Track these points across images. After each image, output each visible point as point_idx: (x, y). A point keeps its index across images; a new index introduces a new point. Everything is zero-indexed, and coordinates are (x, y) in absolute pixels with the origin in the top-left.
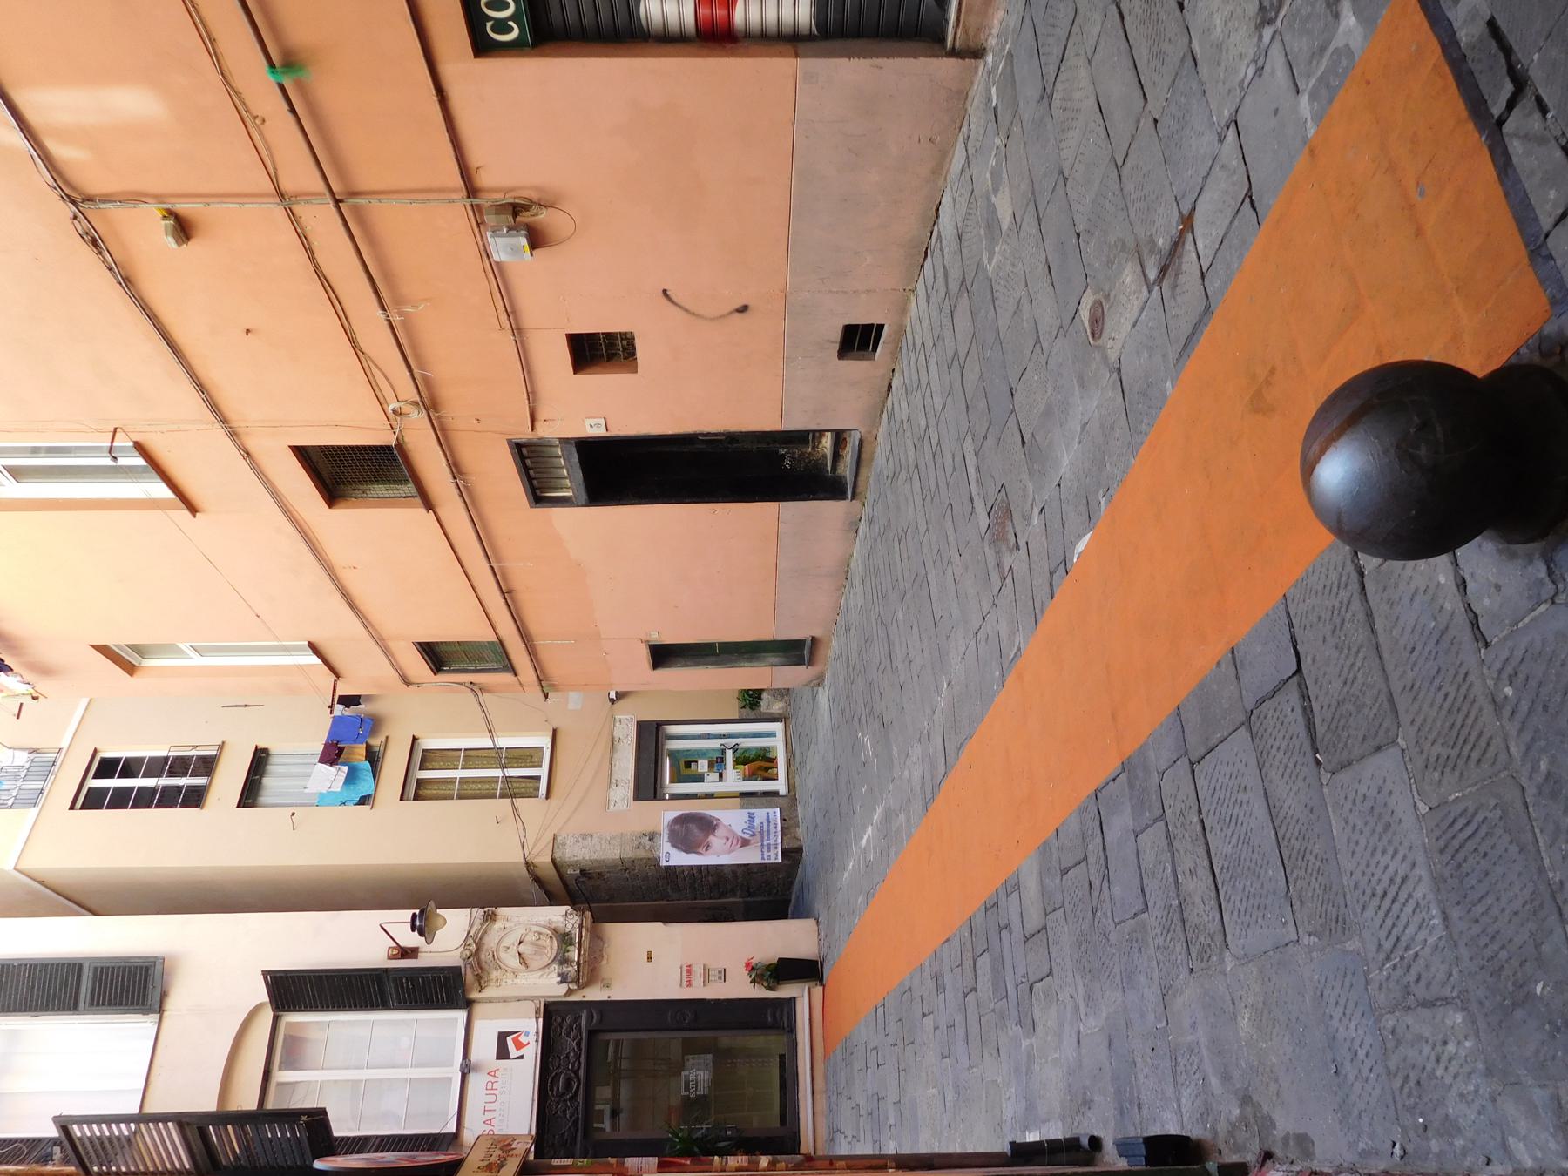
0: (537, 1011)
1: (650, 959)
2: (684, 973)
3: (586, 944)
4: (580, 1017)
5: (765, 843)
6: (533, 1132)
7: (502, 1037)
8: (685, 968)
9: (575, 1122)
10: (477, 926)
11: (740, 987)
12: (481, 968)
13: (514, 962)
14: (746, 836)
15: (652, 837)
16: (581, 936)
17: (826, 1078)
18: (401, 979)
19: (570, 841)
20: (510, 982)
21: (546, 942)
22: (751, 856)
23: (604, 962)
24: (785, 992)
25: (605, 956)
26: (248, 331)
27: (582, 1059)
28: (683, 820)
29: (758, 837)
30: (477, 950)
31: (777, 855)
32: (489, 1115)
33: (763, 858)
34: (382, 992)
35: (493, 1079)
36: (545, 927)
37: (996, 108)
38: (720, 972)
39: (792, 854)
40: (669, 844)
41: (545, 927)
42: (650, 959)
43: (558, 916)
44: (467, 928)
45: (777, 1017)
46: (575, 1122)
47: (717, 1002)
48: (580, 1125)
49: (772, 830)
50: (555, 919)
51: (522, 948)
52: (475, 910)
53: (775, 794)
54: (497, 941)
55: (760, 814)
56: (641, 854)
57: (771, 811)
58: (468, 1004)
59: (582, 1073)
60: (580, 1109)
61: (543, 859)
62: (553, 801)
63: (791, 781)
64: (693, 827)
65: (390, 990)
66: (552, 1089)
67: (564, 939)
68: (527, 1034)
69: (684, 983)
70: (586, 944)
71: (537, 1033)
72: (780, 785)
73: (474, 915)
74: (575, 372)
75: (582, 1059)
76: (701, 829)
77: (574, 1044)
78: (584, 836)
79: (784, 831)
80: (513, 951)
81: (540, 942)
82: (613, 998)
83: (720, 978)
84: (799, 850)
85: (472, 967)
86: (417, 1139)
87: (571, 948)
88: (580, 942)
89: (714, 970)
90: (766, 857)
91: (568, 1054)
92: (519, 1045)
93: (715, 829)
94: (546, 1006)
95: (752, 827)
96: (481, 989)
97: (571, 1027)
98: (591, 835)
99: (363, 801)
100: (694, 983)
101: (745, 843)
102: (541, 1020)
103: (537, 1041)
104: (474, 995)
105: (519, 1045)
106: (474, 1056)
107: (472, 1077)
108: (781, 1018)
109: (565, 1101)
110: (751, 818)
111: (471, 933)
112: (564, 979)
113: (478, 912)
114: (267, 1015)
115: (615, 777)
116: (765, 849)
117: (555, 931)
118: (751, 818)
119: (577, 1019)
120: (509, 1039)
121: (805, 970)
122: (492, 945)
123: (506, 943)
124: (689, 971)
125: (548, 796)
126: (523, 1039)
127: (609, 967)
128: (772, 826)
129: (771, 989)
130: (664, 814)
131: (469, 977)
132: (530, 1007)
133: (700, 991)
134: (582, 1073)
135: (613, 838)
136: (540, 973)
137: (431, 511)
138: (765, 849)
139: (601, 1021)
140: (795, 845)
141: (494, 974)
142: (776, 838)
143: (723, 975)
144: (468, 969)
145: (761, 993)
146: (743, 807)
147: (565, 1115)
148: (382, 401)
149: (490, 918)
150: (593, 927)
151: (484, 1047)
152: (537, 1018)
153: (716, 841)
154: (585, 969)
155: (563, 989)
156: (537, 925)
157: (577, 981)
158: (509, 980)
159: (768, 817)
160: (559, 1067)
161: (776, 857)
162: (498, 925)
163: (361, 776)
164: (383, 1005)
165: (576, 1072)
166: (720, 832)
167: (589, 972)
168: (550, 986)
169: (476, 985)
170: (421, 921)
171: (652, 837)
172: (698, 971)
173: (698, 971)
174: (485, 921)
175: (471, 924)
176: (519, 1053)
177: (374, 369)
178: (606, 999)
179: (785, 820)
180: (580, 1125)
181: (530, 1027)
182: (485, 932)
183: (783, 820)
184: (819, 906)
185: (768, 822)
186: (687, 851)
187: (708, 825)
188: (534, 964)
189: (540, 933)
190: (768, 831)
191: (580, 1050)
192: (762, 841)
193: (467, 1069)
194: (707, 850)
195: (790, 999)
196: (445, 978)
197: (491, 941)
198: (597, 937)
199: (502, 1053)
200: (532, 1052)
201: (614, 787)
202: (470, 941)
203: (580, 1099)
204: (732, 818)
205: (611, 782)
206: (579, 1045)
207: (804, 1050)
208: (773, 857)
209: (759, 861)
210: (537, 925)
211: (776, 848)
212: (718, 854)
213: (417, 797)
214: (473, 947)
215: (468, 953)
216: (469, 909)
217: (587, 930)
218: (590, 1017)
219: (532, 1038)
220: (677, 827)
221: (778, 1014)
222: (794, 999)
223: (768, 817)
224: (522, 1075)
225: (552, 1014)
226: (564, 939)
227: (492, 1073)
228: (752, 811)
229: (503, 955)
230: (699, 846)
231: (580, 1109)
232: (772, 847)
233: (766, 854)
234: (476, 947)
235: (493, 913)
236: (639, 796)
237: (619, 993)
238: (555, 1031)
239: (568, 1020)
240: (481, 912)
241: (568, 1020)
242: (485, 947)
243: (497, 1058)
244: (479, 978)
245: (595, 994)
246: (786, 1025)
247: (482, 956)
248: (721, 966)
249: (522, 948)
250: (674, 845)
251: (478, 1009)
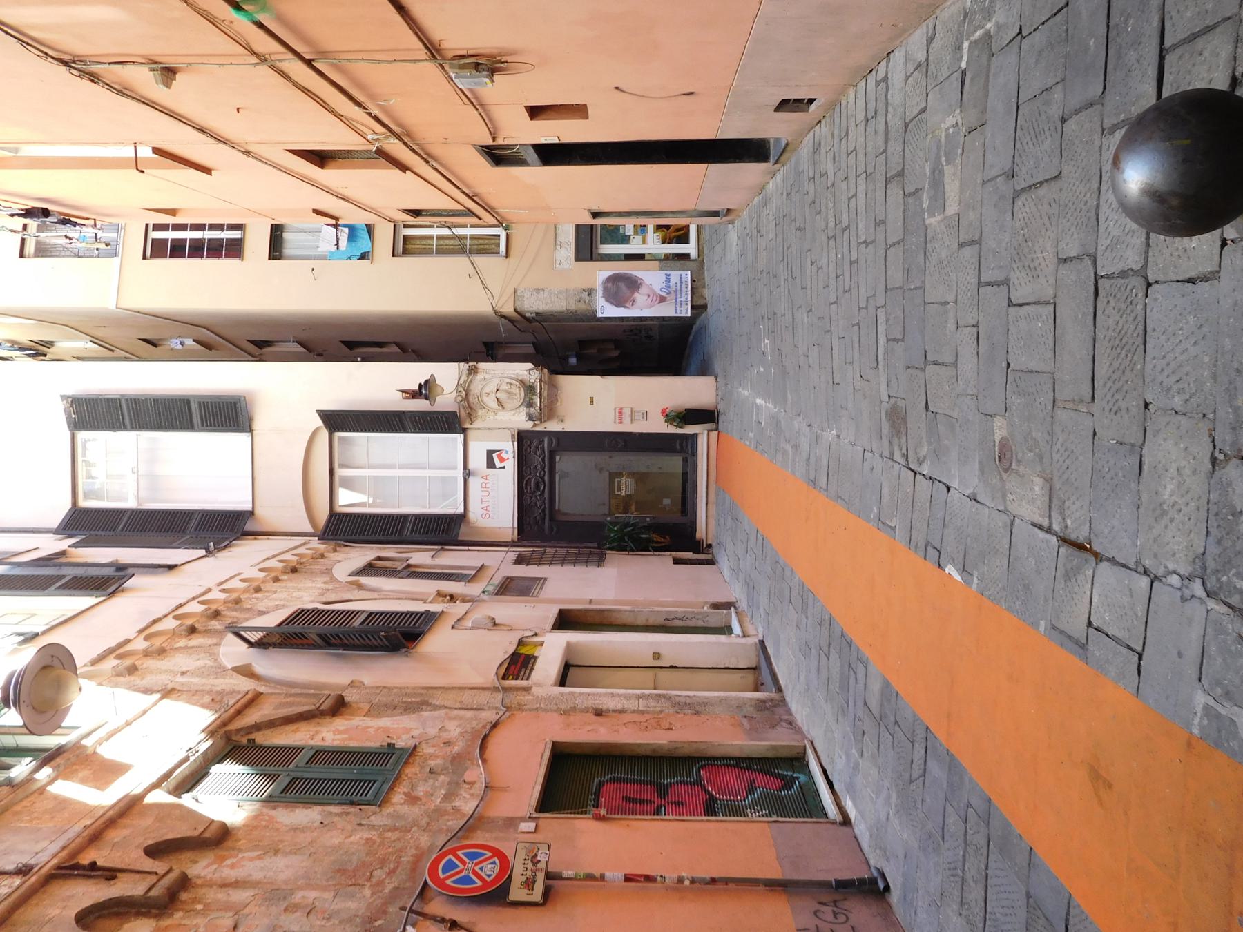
0: (513, 437)
1: (592, 402)
2: (617, 414)
3: (545, 394)
4: (543, 440)
5: (679, 300)
6: (516, 525)
7: (490, 454)
8: (617, 411)
9: (544, 511)
10: (464, 378)
11: (658, 425)
12: (470, 408)
13: (494, 405)
14: (664, 294)
15: (590, 292)
16: (541, 389)
17: (717, 495)
18: (415, 417)
19: (527, 294)
20: (491, 417)
21: (515, 390)
22: (666, 311)
23: (559, 404)
24: (689, 430)
25: (559, 400)
26: (238, 109)
27: (546, 470)
28: (615, 279)
29: (673, 296)
30: (466, 395)
31: (687, 309)
32: (485, 504)
33: (676, 313)
34: (402, 423)
35: (486, 481)
36: (513, 379)
37: (964, 73)
38: (643, 414)
39: (699, 308)
40: (603, 299)
41: (513, 379)
42: (592, 402)
43: (524, 370)
44: (457, 377)
45: (685, 446)
46: (544, 511)
47: (641, 434)
48: (547, 512)
49: (684, 289)
50: (521, 373)
51: (498, 395)
52: (462, 364)
53: (685, 257)
54: (480, 388)
55: (675, 276)
56: (582, 307)
57: (683, 273)
58: (464, 431)
59: (546, 478)
60: (546, 501)
61: (508, 309)
62: (511, 259)
63: (701, 248)
64: (622, 286)
65: (407, 422)
66: (526, 488)
67: (530, 389)
68: (507, 452)
69: (617, 421)
70: (545, 394)
71: (514, 452)
72: (691, 248)
73: (461, 368)
74: (531, 119)
75: (546, 470)
76: (629, 287)
77: (540, 459)
78: (538, 290)
79: (693, 290)
80: (493, 396)
81: (511, 390)
82: (566, 430)
83: (643, 418)
84: (705, 307)
85: (464, 408)
86: (439, 519)
87: (534, 397)
88: (540, 392)
89: (639, 412)
90: (678, 311)
91: (536, 466)
92: (502, 460)
93: (639, 287)
94: (518, 433)
95: (668, 286)
96: (472, 422)
97: (537, 447)
98: (543, 290)
99: (363, 257)
100: (624, 421)
101: (663, 300)
102: (516, 443)
103: (514, 457)
104: (467, 426)
105: (502, 460)
106: (471, 466)
107: (471, 480)
108: (687, 446)
109: (536, 496)
110: (668, 278)
111: (461, 382)
112: (531, 418)
113: (464, 366)
114: (325, 434)
115: (559, 239)
116: (678, 306)
117: (522, 382)
118: (668, 278)
119: (541, 442)
120: (495, 455)
121: (706, 416)
122: (476, 391)
123: (487, 390)
124: (621, 413)
125: (507, 256)
126: (504, 455)
127: (562, 407)
128: (684, 286)
129: (678, 426)
130: (600, 273)
131: (463, 414)
132: (508, 434)
133: (628, 427)
134: (546, 478)
135: (560, 292)
136: (513, 412)
137: (407, 172)
138: (678, 306)
139: (558, 444)
140: (700, 302)
141: (480, 412)
142: (687, 297)
143: (645, 415)
144: (462, 409)
145: (672, 430)
146: (661, 269)
147: (536, 505)
148: (361, 133)
149: (473, 371)
150: (549, 378)
151: (478, 460)
152: (513, 442)
153: (640, 297)
154: (545, 411)
155: (531, 423)
156: (508, 377)
157: (541, 420)
158: (491, 416)
159: (681, 278)
160: (530, 474)
161: (686, 312)
162: (480, 376)
163: (359, 234)
164: (404, 430)
165: (542, 478)
166: (643, 290)
167: (549, 411)
168: (521, 421)
169: (468, 420)
170: (425, 390)
171: (590, 292)
172: (627, 412)
173: (627, 412)
174: (470, 374)
175: (460, 376)
176: (502, 465)
177: (356, 125)
178: (561, 430)
179: (694, 281)
180: (547, 512)
181: (509, 448)
182: (471, 381)
183: (693, 281)
184: (718, 366)
185: (681, 282)
186: (618, 305)
187: (633, 284)
188: (507, 406)
189: (511, 384)
190: (681, 290)
191: (544, 463)
192: (676, 298)
193: (467, 473)
194: (632, 305)
195: (694, 434)
196: (446, 418)
197: (476, 388)
198: (553, 386)
199: (491, 464)
200: (511, 464)
201: (558, 247)
202: (460, 389)
203: (546, 495)
204: (652, 278)
205: (556, 244)
206: (543, 460)
207: (702, 476)
208: (684, 311)
209: (673, 314)
210: (508, 377)
211: (687, 304)
212: (641, 308)
213: (405, 252)
214: (463, 394)
215: (460, 398)
216: (457, 364)
217: (545, 383)
218: (550, 442)
219: (510, 455)
220: (610, 285)
221: (684, 444)
222: (697, 434)
223: (681, 278)
224: (505, 481)
225: (522, 438)
226: (530, 389)
227: (485, 477)
228: (668, 273)
229: (485, 399)
230: (626, 301)
231: (546, 501)
232: (684, 304)
233: (679, 309)
234: (465, 392)
235: (475, 367)
236: (579, 257)
237: (572, 425)
238: (526, 450)
239: (535, 442)
240: (467, 366)
241: (535, 442)
242: (472, 393)
243: (488, 467)
244: (469, 415)
245: (553, 426)
246: (690, 452)
247: (471, 400)
248: (644, 410)
249: (498, 395)
250: (607, 300)
251: (471, 434)
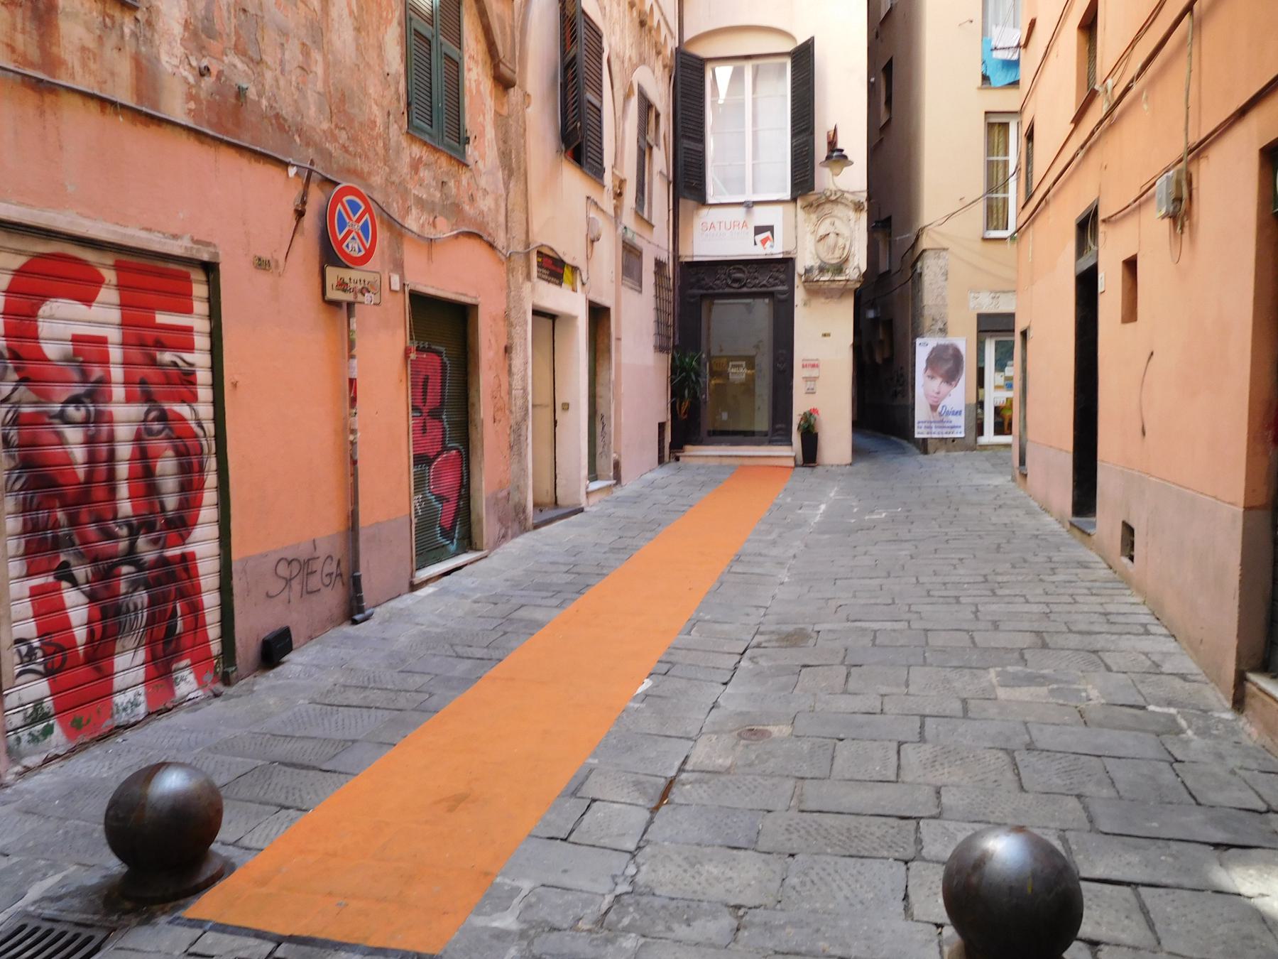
0: (788, 253)
1: (825, 335)
2: (812, 362)
5: (933, 425)
6: (696, 259)
7: (770, 229)
8: (816, 363)
9: (711, 288)
10: (850, 197)
12: (818, 206)
13: (822, 232)
14: (939, 409)
15: (943, 331)
19: (942, 263)
21: (837, 253)
22: (921, 412)
23: (823, 300)
24: (796, 438)
25: (827, 301)
28: (957, 357)
29: (938, 419)
30: (832, 201)
31: (922, 433)
32: (717, 226)
33: (919, 422)
35: (741, 225)
37: (1143, 708)
39: (923, 446)
40: (935, 345)
42: (825, 335)
43: (859, 262)
44: (851, 190)
45: (779, 432)
46: (711, 288)
47: (791, 388)
49: (945, 430)
50: (856, 258)
53: (980, 431)
54: (839, 215)
55: (960, 421)
56: (927, 322)
57: (962, 429)
58: (794, 200)
59: (745, 290)
61: (925, 243)
62: (980, 246)
63: (989, 447)
64: (949, 365)
65: (802, 138)
66: (734, 269)
67: (839, 269)
69: (805, 363)
70: (834, 285)
72: (989, 437)
76: (947, 372)
78: (946, 274)
79: (943, 440)
80: (831, 229)
84: (925, 452)
87: (830, 274)
88: (834, 281)
89: (815, 385)
90: (920, 424)
92: (764, 242)
93: (947, 382)
95: (948, 413)
96: (804, 208)
98: (946, 279)
99: (985, 78)
100: (805, 369)
101: (934, 408)
104: (799, 203)
106: (757, 209)
107: (742, 210)
108: (778, 435)
110: (958, 413)
112: (808, 271)
113: (863, 197)
114: (789, 47)
115: (1002, 296)
116: (927, 424)
117: (846, 260)
118: (958, 413)
119: (782, 283)
120: (768, 234)
121: (810, 454)
122: (836, 212)
124: (813, 366)
125: (985, 240)
126: (768, 244)
127: (819, 303)
128: (949, 430)
130: (963, 340)
131: (811, 198)
132: (790, 248)
135: (943, 298)
136: (814, 252)
138: (927, 424)
140: (930, 448)
141: (814, 217)
142: (936, 434)
143: (811, 392)
146: (967, 406)
149: (858, 207)
150: (850, 289)
151: (763, 216)
152: (783, 253)
153: (937, 384)
154: (815, 286)
155: (802, 272)
156: (851, 246)
157: (805, 282)
158: (810, 228)
159: (957, 427)
161: (919, 433)
162: (852, 214)
163: (1010, 72)
164: (794, 135)
166: (945, 387)
167: (815, 290)
169: (805, 204)
170: (836, 156)
171: (943, 331)
172: (814, 373)
173: (814, 373)
175: (853, 193)
176: (758, 242)
177: (1124, 64)
179: (953, 441)
181: (775, 249)
182: (846, 205)
183: (954, 440)
184: (863, 466)
185: (952, 427)
186: (928, 360)
187: (951, 377)
188: (821, 246)
189: (844, 248)
190: (944, 427)
191: (761, 287)
192: (935, 422)
193: (749, 205)
194: (929, 376)
195: (791, 441)
196: (806, 181)
197: (839, 211)
198: (842, 293)
199: (759, 230)
200: (759, 252)
201: (992, 295)
202: (839, 194)
203: (727, 290)
204: (958, 396)
205: (996, 293)
206: (764, 286)
207: (748, 451)
208: (920, 430)
209: (917, 418)
211: (928, 433)
212: (924, 386)
213: (990, 126)
214: (833, 198)
215: (828, 194)
216: (865, 188)
220: (951, 351)
223: (957, 427)
224: (743, 246)
225: (787, 263)
226: (839, 269)
227: (745, 224)
228: (963, 413)
229: (828, 221)
230: (933, 369)
232: (928, 430)
233: (923, 425)
234: (835, 200)
235: (861, 210)
236: (982, 318)
238: (774, 267)
241: (782, 276)
244: (811, 205)
245: (799, 295)
247: (828, 206)
249: (832, 236)
250: (934, 349)
251: (791, 207)
